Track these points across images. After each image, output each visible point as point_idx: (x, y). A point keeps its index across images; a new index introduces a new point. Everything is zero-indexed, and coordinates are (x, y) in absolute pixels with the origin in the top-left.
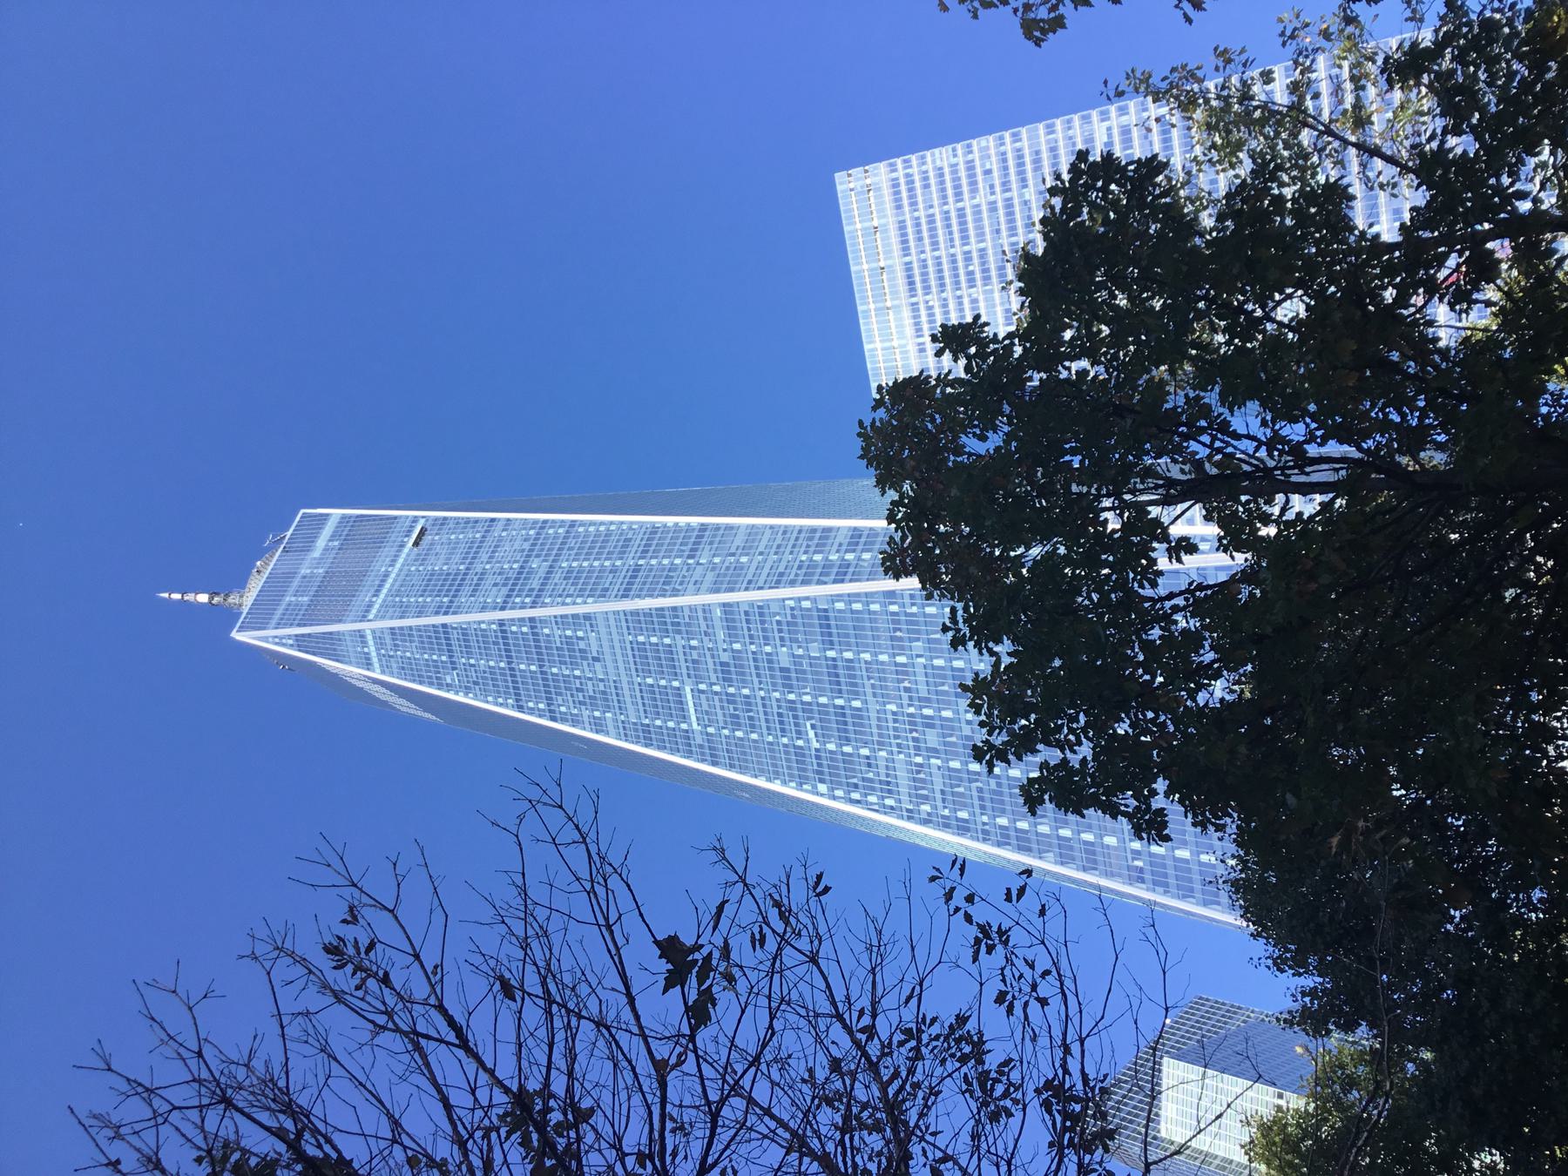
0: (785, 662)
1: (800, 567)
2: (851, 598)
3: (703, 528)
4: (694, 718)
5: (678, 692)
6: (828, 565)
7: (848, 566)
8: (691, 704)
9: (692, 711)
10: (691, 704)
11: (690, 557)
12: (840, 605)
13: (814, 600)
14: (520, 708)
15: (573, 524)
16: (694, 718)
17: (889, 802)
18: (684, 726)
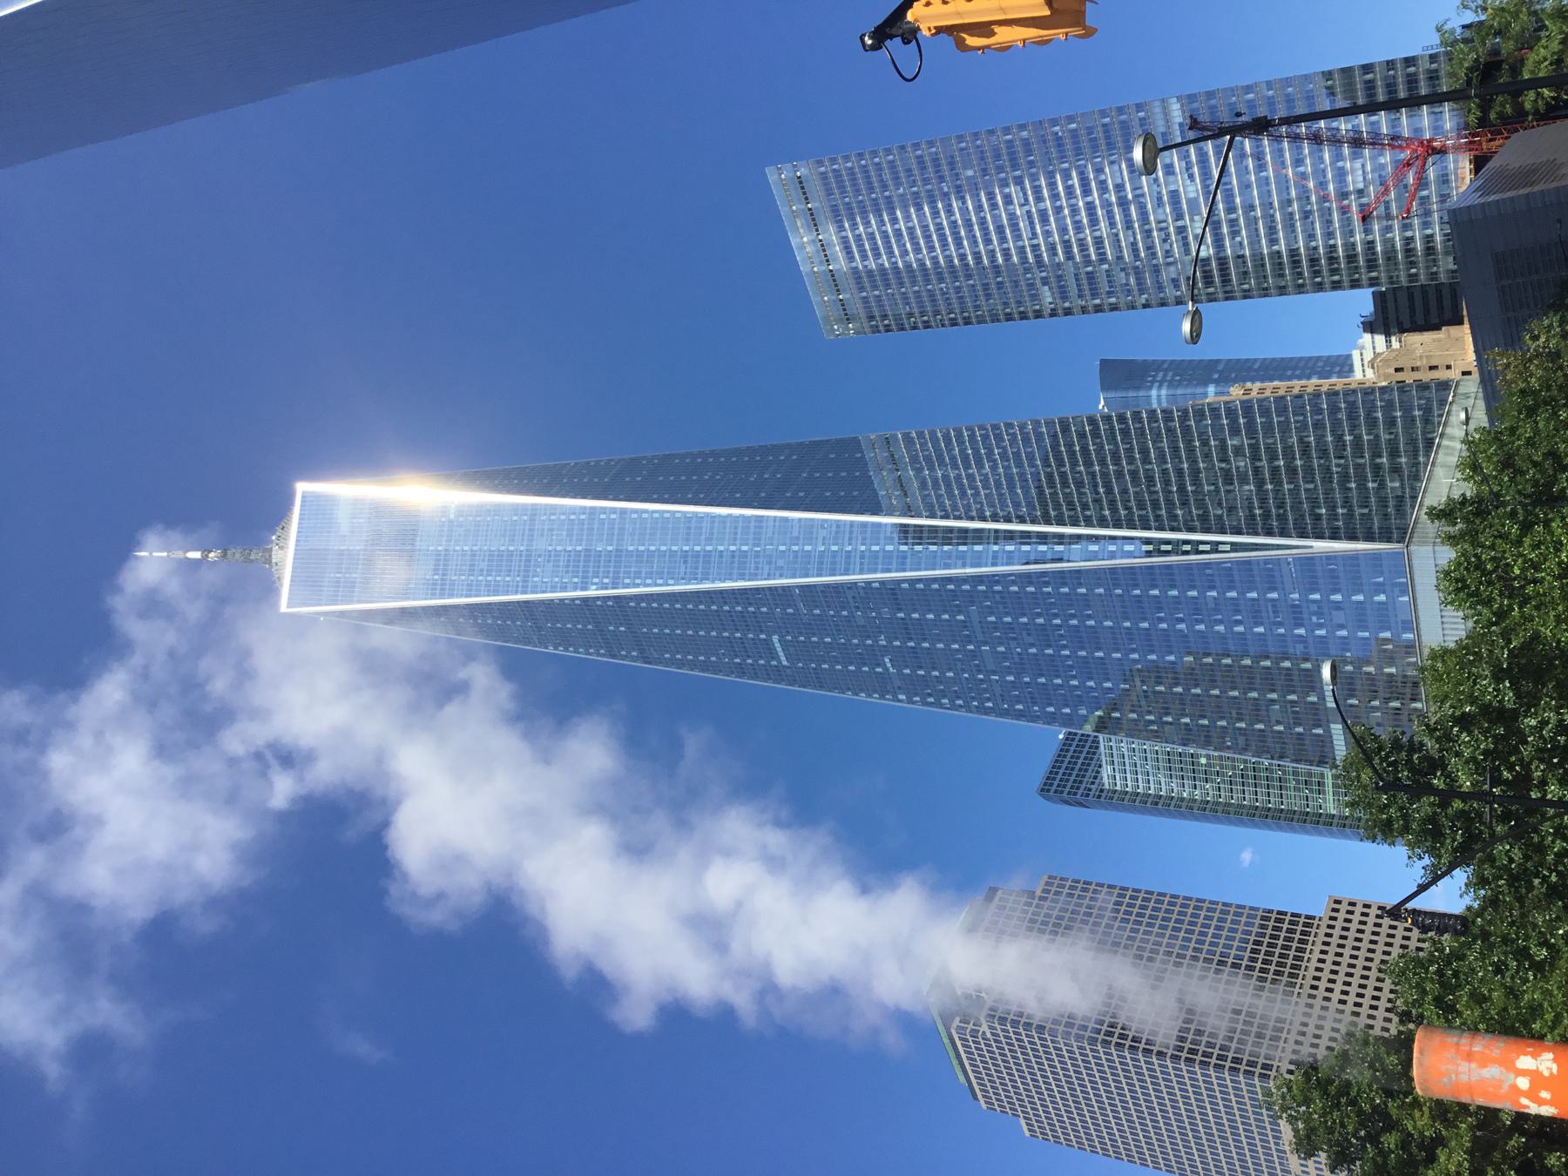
0: (862, 622)
1: (862, 557)
2: (913, 582)
3: (759, 519)
4: (783, 658)
5: (768, 642)
6: (888, 555)
7: (905, 558)
8: (779, 649)
9: (781, 654)
10: (779, 649)
11: (755, 545)
12: (905, 586)
13: (882, 583)
14: (613, 656)
15: (623, 512)
16: (783, 658)
17: (960, 702)
18: (774, 663)
